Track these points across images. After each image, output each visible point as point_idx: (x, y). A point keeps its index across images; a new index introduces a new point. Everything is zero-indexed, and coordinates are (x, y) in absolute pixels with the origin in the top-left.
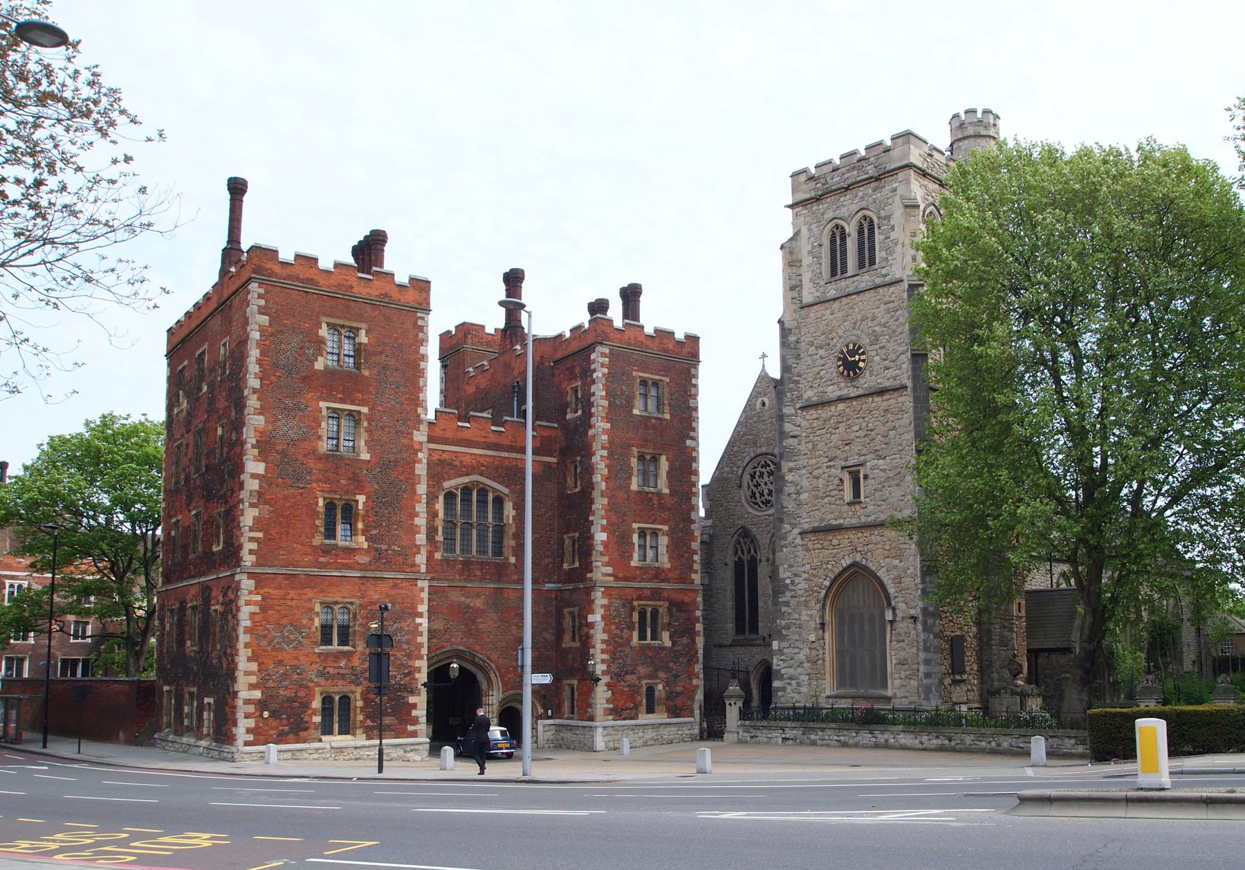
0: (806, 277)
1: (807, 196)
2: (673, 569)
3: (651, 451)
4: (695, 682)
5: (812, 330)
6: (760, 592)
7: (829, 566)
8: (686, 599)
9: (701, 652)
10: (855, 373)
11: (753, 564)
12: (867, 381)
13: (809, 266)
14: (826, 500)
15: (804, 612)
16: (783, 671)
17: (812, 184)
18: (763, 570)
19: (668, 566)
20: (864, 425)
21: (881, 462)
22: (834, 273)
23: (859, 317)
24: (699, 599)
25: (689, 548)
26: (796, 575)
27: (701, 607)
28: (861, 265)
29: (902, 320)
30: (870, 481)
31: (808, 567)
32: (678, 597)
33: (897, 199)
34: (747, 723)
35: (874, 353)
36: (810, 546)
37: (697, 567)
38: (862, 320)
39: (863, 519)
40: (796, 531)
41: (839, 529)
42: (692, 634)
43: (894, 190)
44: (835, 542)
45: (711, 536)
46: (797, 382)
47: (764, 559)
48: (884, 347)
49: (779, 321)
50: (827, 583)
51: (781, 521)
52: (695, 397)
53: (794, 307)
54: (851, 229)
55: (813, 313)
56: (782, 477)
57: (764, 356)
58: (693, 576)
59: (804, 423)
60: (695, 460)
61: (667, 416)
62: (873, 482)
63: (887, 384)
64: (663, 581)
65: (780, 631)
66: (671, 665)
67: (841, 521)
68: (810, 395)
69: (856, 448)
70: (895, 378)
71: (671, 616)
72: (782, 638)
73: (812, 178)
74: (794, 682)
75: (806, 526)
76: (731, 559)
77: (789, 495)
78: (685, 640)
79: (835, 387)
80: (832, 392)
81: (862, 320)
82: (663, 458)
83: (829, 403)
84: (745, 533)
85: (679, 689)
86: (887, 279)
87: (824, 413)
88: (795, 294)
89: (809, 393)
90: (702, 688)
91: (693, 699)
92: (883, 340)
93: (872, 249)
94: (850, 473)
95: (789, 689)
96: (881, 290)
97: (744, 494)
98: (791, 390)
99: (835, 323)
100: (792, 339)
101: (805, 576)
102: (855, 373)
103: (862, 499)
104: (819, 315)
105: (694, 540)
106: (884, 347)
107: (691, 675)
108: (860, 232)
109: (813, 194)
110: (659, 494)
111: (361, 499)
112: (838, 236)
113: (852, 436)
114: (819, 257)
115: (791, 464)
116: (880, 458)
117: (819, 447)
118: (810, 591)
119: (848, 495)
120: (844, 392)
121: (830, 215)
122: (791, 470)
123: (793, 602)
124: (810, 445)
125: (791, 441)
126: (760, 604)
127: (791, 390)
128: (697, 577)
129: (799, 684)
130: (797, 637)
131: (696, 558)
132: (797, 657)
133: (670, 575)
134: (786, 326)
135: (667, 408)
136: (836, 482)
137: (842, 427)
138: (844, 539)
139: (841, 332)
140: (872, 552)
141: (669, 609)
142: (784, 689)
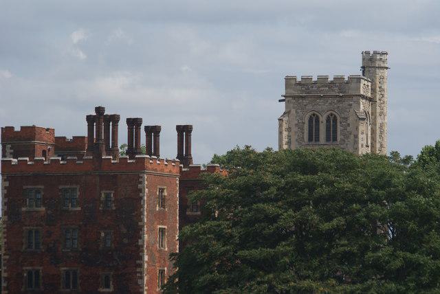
13: (296, 133)
22: (310, 139)
28: (328, 139)
43: (351, 105)
54: (323, 119)
93: (335, 132)
108: (328, 120)
111: (166, 269)
112: (314, 121)
114: (302, 129)
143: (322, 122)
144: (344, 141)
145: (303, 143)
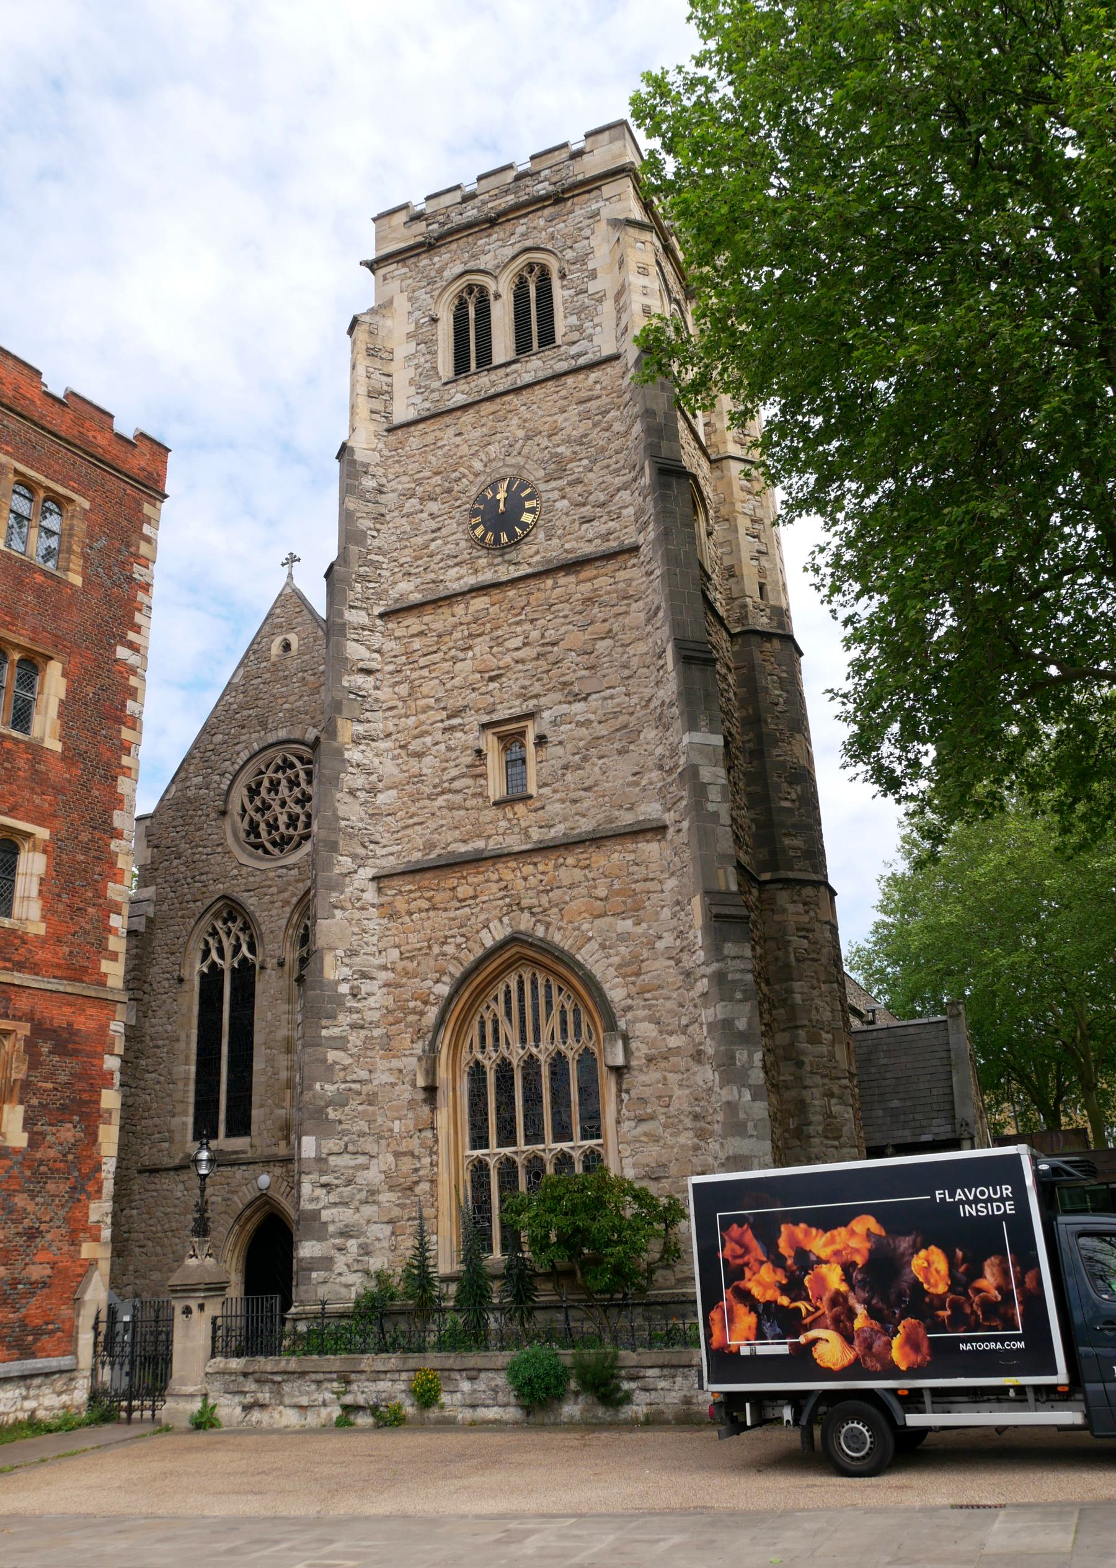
0: (402, 376)
1: (411, 242)
2: (54, 938)
3: (24, 642)
4: (87, 1250)
5: (412, 467)
6: (258, 1038)
7: (450, 949)
8: (84, 1023)
9: (109, 1166)
10: (512, 535)
11: (245, 975)
12: (537, 551)
13: (408, 358)
14: (441, 801)
15: (382, 1064)
16: (326, 1215)
17: (421, 227)
18: (269, 988)
19: (39, 929)
20: (535, 635)
21: (578, 707)
22: (461, 366)
23: (521, 433)
24: (117, 1027)
25: (101, 894)
26: (365, 976)
27: (119, 1048)
28: (523, 346)
29: (617, 427)
30: (552, 750)
31: (395, 954)
32: (59, 1016)
33: (602, 227)
34: (235, 1364)
35: (556, 495)
36: (400, 904)
37: (117, 944)
38: (528, 438)
39: (536, 834)
40: (367, 872)
41: (476, 860)
42: (89, 1117)
44: (463, 891)
45: (150, 921)
46: (377, 566)
47: (271, 963)
48: (579, 481)
49: (344, 452)
50: (444, 990)
51: (334, 847)
52: (147, 562)
53: (372, 427)
55: (414, 440)
56: (339, 752)
57: (293, 559)
58: (106, 966)
59: (390, 645)
60: (133, 693)
61: (77, 580)
62: (559, 750)
63: (587, 549)
64: (20, 966)
65: (321, 1111)
66: (20, 1201)
67: (480, 844)
68: (408, 589)
69: (513, 683)
70: (605, 537)
71: (34, 1065)
72: (323, 1126)
73: (418, 217)
74: (352, 1245)
75: (390, 863)
76: (196, 968)
77: (352, 793)
78: (68, 1133)
79: (463, 571)
80: (457, 579)
81: (528, 438)
82: (54, 669)
83: (450, 599)
84: (232, 910)
85: (37, 1272)
86: (582, 361)
87: (439, 620)
88: (378, 405)
89: (404, 586)
90: (105, 1266)
91: (76, 1302)
92: (577, 468)
94: (501, 738)
95: (341, 1261)
96: (570, 380)
97: (232, 828)
98: (364, 578)
99: (464, 449)
100: (369, 483)
101: (384, 976)
102: (512, 535)
103: (532, 789)
104: (430, 439)
105: (116, 876)
106: (579, 481)
107: (78, 1230)
109: (420, 239)
110: (36, 750)
113: (507, 659)
114: (429, 343)
115: (360, 728)
116: (577, 698)
117: (425, 690)
118: (396, 1014)
119: (496, 788)
120: (487, 576)
121: (459, 269)
122: (356, 742)
123: (355, 1039)
124: (403, 689)
125: (360, 680)
126: (258, 1065)
127: (364, 578)
128: (114, 972)
129: (366, 1250)
130: (363, 1125)
131: (117, 921)
132: (363, 1177)
133: (41, 955)
134: (360, 456)
135: (76, 563)
136: (468, 758)
137: (481, 646)
138: (487, 884)
139: (478, 465)
140: (561, 905)
141: (30, 1045)
142: (326, 1263)
143: (497, 296)
144: (579, 329)
145: (436, 384)
